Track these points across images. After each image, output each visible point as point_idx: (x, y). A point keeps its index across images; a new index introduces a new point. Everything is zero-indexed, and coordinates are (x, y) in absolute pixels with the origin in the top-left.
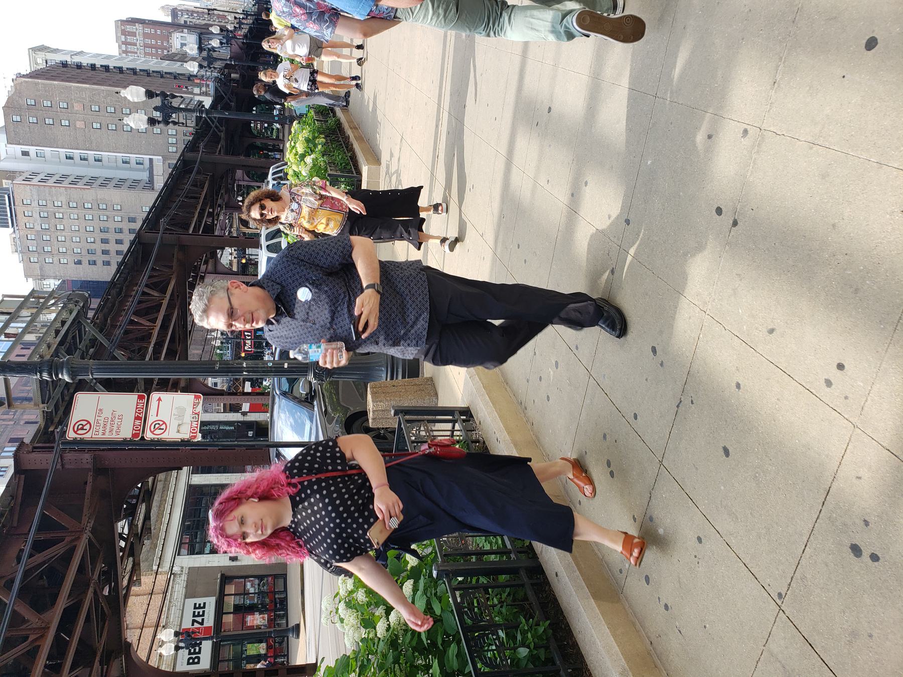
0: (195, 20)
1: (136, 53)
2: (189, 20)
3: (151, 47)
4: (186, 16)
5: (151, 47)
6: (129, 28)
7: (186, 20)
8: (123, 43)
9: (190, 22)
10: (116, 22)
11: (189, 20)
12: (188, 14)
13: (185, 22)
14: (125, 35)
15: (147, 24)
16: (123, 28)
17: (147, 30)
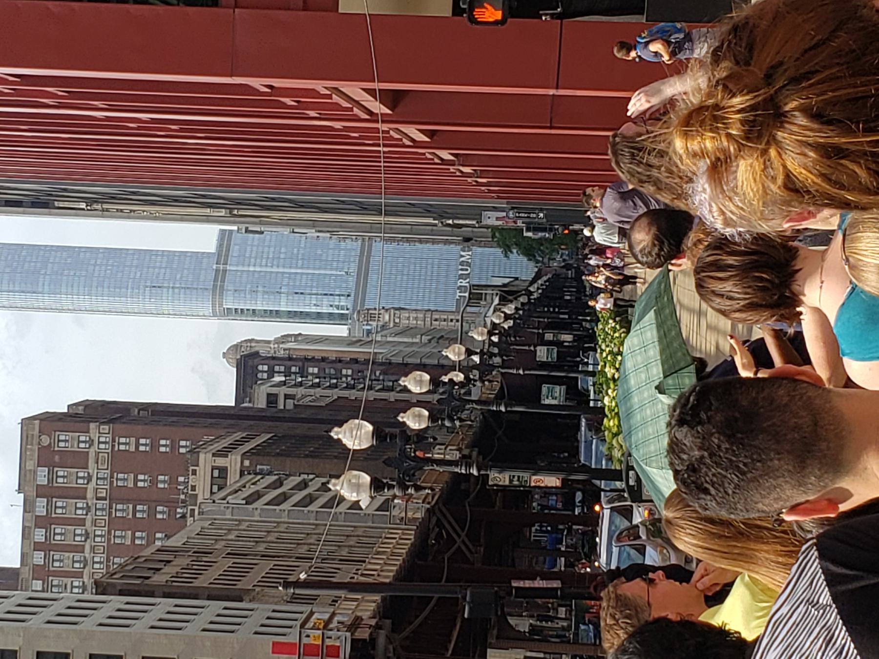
0: (300, 391)
1: (81, 522)
2: (283, 390)
3: (133, 497)
4: (278, 379)
5: (133, 497)
6: (67, 441)
7: (274, 390)
8: (41, 491)
9: (287, 397)
10: (26, 423)
11: (283, 390)
12: (287, 373)
13: (272, 399)
14: (51, 466)
15: (136, 421)
16: (46, 440)
17: (126, 444)
